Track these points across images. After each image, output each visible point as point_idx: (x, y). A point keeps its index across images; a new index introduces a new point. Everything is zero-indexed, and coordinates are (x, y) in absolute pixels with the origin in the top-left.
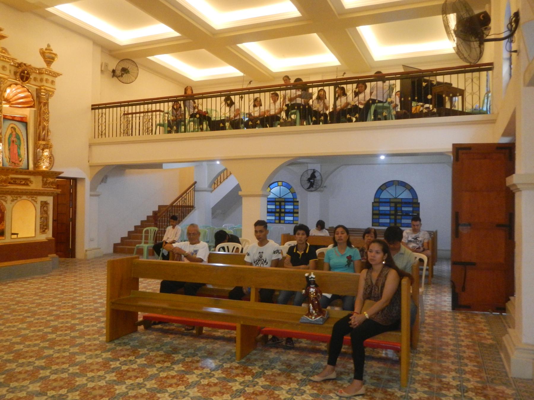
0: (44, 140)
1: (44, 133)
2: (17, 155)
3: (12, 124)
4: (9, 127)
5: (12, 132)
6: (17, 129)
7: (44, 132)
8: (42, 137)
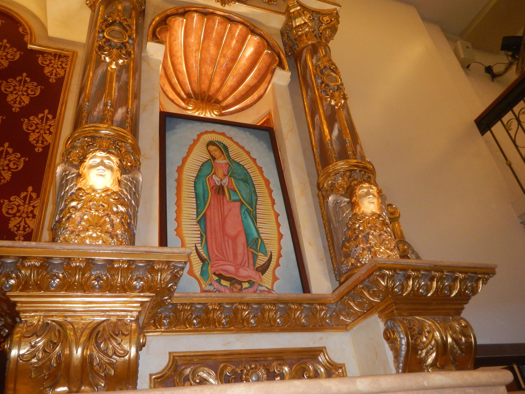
0: (343, 155)
1: (336, 132)
2: (241, 240)
3: (213, 132)
4: (196, 142)
5: (214, 158)
6: (233, 150)
7: (336, 126)
8: (334, 147)
